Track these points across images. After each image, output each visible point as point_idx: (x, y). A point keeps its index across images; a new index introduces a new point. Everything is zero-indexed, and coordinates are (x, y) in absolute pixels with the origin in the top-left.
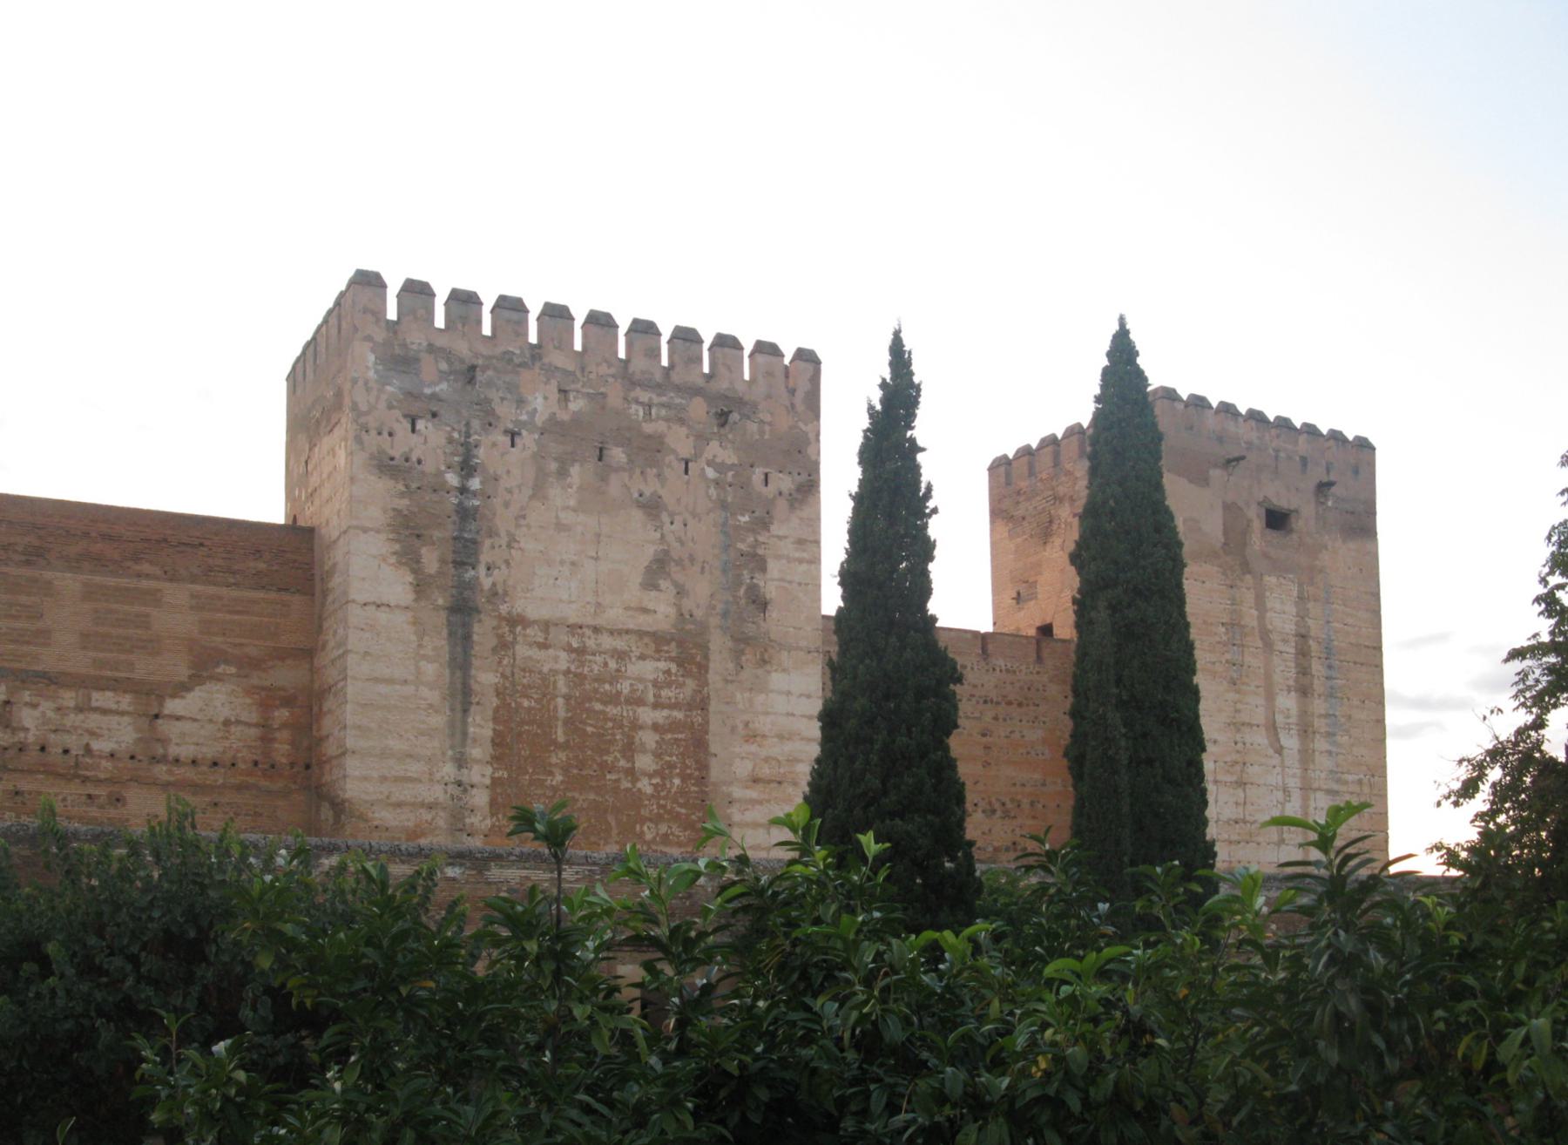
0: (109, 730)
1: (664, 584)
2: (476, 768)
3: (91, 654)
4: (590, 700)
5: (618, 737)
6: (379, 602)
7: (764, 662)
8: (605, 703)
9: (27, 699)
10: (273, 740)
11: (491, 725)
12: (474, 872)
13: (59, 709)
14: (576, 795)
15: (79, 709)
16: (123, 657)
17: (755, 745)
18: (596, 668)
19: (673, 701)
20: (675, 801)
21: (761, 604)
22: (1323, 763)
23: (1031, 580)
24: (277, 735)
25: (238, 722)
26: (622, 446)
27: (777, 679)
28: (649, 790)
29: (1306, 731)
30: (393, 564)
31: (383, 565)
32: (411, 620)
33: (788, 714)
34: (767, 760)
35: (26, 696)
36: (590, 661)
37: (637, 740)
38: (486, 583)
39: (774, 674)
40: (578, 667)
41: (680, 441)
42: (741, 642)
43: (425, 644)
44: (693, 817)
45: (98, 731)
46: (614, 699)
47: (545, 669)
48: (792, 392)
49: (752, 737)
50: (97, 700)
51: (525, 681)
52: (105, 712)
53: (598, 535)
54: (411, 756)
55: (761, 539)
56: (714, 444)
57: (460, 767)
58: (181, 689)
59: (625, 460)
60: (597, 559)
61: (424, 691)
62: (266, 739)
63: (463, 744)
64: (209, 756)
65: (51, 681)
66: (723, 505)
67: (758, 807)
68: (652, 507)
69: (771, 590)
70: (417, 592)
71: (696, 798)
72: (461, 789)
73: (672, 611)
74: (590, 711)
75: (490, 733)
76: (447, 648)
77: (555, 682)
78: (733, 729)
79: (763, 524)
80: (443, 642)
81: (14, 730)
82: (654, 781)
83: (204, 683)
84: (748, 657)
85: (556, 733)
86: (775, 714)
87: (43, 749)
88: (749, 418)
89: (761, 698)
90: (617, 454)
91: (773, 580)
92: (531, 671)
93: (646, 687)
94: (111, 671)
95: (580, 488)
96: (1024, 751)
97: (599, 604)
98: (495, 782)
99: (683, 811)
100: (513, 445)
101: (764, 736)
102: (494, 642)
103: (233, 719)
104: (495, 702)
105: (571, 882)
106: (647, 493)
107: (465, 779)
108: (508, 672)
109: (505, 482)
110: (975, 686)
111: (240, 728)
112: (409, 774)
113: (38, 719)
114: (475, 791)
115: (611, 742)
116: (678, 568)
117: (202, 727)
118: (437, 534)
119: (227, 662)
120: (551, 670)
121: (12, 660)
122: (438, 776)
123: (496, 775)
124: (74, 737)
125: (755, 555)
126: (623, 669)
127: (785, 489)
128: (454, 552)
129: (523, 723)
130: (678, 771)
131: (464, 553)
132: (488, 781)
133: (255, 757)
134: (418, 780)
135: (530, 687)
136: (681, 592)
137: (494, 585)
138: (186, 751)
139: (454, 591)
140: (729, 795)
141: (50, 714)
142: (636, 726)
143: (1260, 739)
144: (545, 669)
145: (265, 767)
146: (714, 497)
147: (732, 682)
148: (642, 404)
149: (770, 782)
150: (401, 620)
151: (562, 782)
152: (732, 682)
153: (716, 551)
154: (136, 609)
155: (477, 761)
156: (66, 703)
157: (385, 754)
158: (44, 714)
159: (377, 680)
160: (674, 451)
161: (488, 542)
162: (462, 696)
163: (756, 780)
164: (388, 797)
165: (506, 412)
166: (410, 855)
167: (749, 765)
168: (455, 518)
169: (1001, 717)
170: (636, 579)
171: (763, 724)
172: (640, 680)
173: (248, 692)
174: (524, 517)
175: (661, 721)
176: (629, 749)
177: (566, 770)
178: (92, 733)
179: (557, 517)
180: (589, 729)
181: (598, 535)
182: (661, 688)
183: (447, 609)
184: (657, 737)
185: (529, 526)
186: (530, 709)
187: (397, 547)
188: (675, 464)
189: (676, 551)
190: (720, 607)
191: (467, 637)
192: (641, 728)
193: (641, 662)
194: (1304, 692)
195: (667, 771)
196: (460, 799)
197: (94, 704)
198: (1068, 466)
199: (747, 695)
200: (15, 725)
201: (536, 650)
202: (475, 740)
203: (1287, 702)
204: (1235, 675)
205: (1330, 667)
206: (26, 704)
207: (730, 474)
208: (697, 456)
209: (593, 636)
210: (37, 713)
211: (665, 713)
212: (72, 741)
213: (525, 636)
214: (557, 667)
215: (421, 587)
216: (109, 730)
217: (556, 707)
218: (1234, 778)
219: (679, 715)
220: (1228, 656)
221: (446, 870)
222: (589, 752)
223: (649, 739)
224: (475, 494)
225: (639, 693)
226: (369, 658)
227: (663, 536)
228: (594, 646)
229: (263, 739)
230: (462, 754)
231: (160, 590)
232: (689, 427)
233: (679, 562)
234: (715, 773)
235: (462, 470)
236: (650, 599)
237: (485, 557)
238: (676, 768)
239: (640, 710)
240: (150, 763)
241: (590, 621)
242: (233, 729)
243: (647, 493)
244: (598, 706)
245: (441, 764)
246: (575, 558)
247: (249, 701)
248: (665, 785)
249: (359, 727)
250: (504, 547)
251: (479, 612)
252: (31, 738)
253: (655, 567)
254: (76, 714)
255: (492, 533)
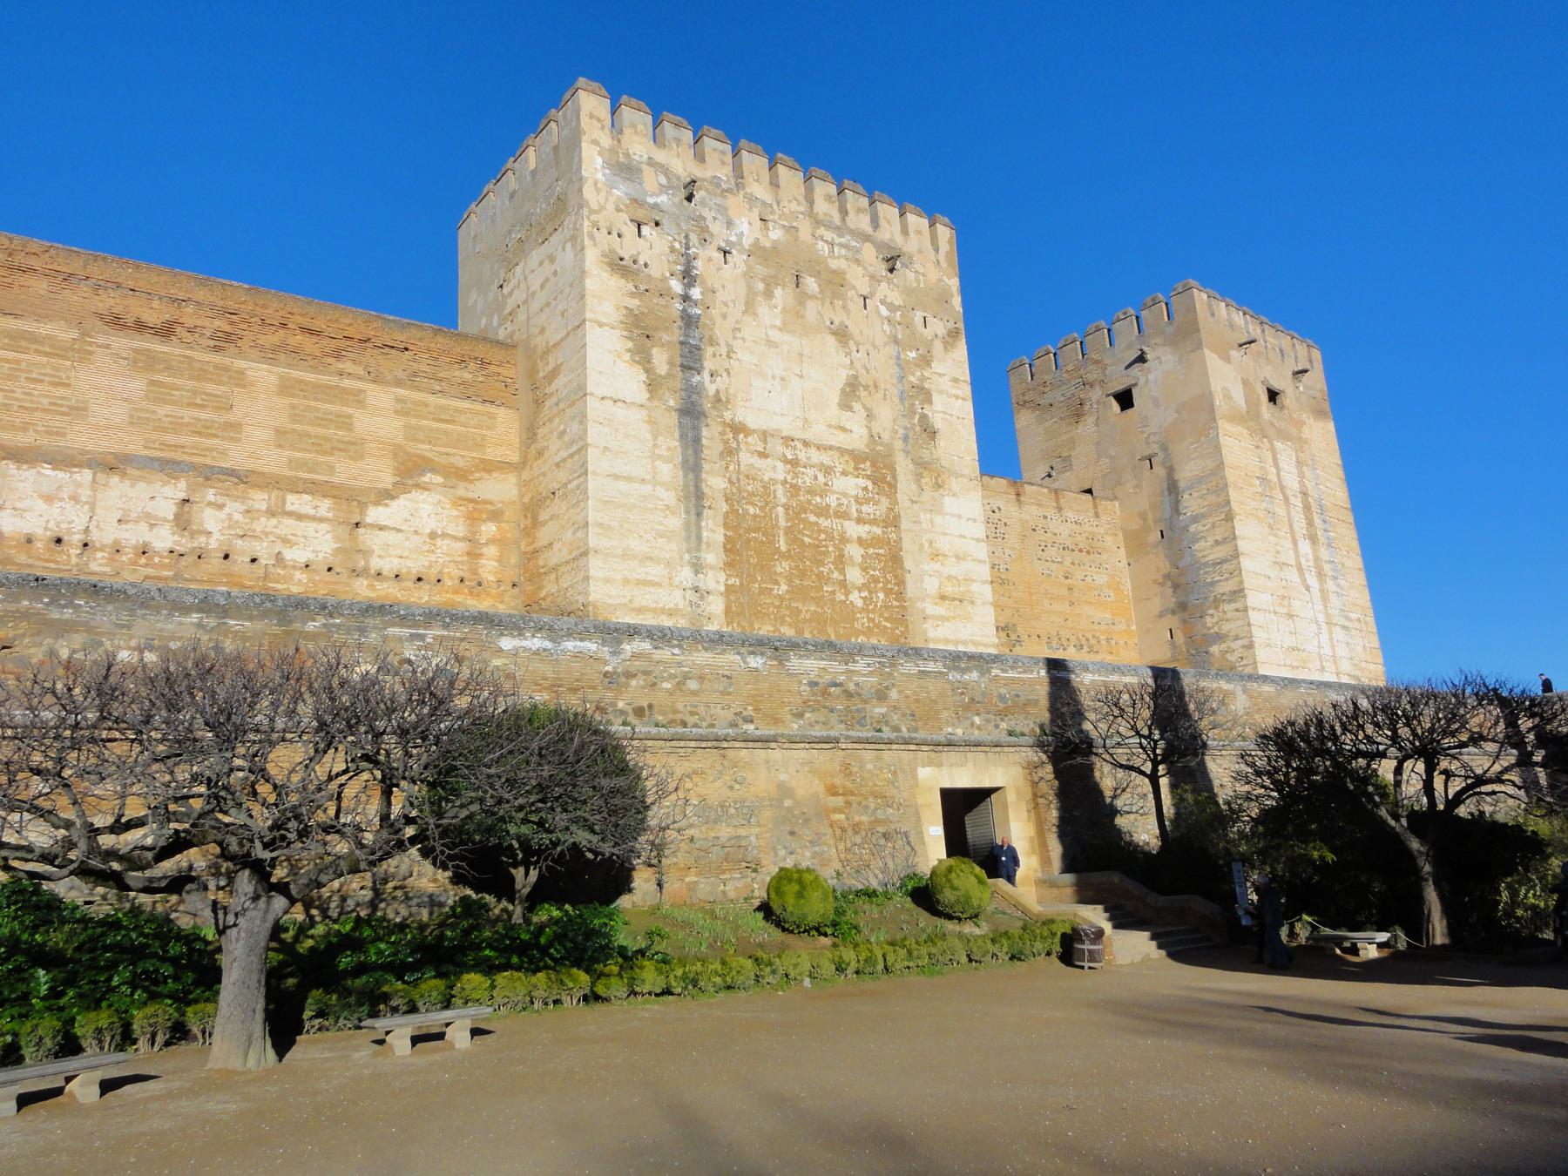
0: (305, 537)
1: (857, 406)
2: (711, 573)
3: (286, 453)
4: (805, 511)
5: (830, 549)
6: (615, 397)
7: (939, 486)
8: (818, 515)
9: (212, 498)
10: (480, 555)
11: (723, 531)
12: (775, 663)
13: (248, 511)
14: (800, 605)
15: (271, 513)
16: (321, 458)
17: (939, 563)
18: (807, 480)
19: (872, 517)
20: (881, 615)
21: (931, 433)
22: (1335, 601)
23: (1064, 455)
24: (485, 550)
25: (445, 535)
26: (814, 277)
27: (949, 503)
28: (859, 603)
29: (1321, 575)
30: (625, 362)
31: (618, 361)
32: (646, 418)
33: (961, 536)
34: (949, 578)
35: (211, 495)
36: (803, 473)
37: (846, 552)
38: (711, 389)
39: (946, 498)
40: (793, 479)
41: (858, 280)
42: (923, 466)
43: (659, 443)
44: (897, 631)
45: (292, 538)
46: (823, 511)
47: (766, 478)
48: (937, 250)
49: (935, 556)
50: (292, 504)
51: (749, 488)
52: (300, 517)
53: (801, 355)
54: (651, 558)
55: (926, 374)
56: (884, 285)
57: (697, 572)
58: (385, 496)
59: (817, 290)
60: (801, 377)
61: (661, 492)
62: (474, 555)
63: (699, 549)
64: (414, 571)
65: (241, 479)
66: (896, 341)
67: (946, 623)
68: (842, 335)
69: (938, 421)
70: (650, 392)
71: (898, 612)
72: (698, 595)
73: (864, 431)
74: (805, 521)
75: (721, 539)
76: (679, 449)
77: (775, 491)
78: (922, 545)
79: (926, 361)
80: (677, 444)
81: (193, 534)
82: (863, 594)
83: (409, 492)
84: (927, 480)
85: (779, 541)
86: (951, 535)
87: (226, 557)
88: (907, 267)
89: (938, 519)
90: (811, 284)
91: (938, 412)
92: (754, 479)
93: (849, 501)
94: (309, 473)
95: (784, 309)
96: (1096, 593)
97: (806, 420)
98: (729, 589)
99: (889, 625)
100: (726, 263)
101: (945, 555)
102: (721, 447)
103: (440, 532)
104: (725, 507)
105: (864, 675)
106: (837, 323)
107: (701, 585)
108: (734, 479)
109: (721, 296)
110: (1055, 534)
111: (447, 541)
112: (650, 578)
113: (223, 521)
114: (711, 598)
115: (826, 553)
116: (866, 393)
117: (407, 539)
118: (666, 337)
119: (433, 471)
120: (771, 479)
121: (195, 454)
122: (676, 581)
123: (730, 582)
124: (265, 545)
125: (923, 388)
126: (830, 483)
127: (940, 335)
128: (681, 356)
129: (749, 530)
130: (881, 585)
131: (690, 360)
132: (722, 589)
133: (462, 574)
134: (658, 585)
135: (753, 494)
136: (870, 416)
137: (718, 391)
138: (388, 565)
139: (683, 393)
140: (923, 611)
141: (238, 517)
142: (844, 540)
143: (1293, 575)
144: (766, 478)
145: (473, 584)
146: (888, 333)
147: (916, 502)
148: (826, 241)
149: (954, 599)
150: (637, 417)
151: (787, 591)
152: (916, 502)
153: (895, 381)
154: (337, 408)
155: (712, 568)
156: (256, 506)
157: (626, 555)
158: (230, 516)
159: (616, 477)
160: (854, 288)
161: (709, 351)
162: (696, 499)
163: (943, 598)
164: (630, 601)
165: (716, 228)
166: (712, 641)
167: (936, 582)
168: (679, 323)
169: (1076, 562)
170: (835, 398)
171: (943, 544)
172: (845, 495)
173: (458, 502)
174: (739, 330)
175: (864, 536)
176: (841, 562)
177: (790, 581)
178: (285, 541)
179: (766, 333)
180: (807, 540)
181: (801, 355)
182: (861, 504)
183: (678, 410)
184: (862, 551)
185: (743, 339)
186: (755, 516)
187: (630, 345)
188: (856, 297)
189: (862, 380)
190: (901, 432)
191: (697, 440)
192: (848, 541)
193: (843, 477)
194: (1313, 540)
195: (872, 585)
196: (698, 606)
197: (289, 507)
198: (1096, 357)
199: (928, 515)
200: (194, 528)
201: (757, 458)
202: (708, 545)
203: (1305, 547)
204: (1271, 521)
205: (1324, 521)
206: (210, 504)
207: (899, 313)
208: (872, 294)
209: (804, 449)
210: (222, 515)
211: (867, 527)
212: (262, 549)
213: (747, 443)
214: (775, 476)
215: (653, 386)
216: (305, 537)
217: (777, 516)
218: (1286, 611)
219: (878, 531)
220: (1264, 505)
221: (748, 659)
222: (808, 563)
223: (854, 552)
224: (696, 303)
225: (844, 507)
226: (607, 453)
227: (852, 362)
228: (805, 460)
229: (468, 554)
230: (698, 559)
231: (361, 391)
232: (865, 269)
233: (866, 388)
234: (910, 590)
235: (684, 278)
236: (846, 418)
237: (708, 364)
238: (879, 582)
239: (847, 523)
240: (350, 577)
241: (798, 434)
242: (439, 542)
243: (837, 323)
244: (812, 518)
245: (679, 568)
246: (784, 374)
247: (455, 513)
248: (872, 598)
249: (602, 524)
250: (724, 356)
251: (706, 416)
252: (213, 544)
253: (848, 390)
254: (268, 519)
255: (712, 342)
